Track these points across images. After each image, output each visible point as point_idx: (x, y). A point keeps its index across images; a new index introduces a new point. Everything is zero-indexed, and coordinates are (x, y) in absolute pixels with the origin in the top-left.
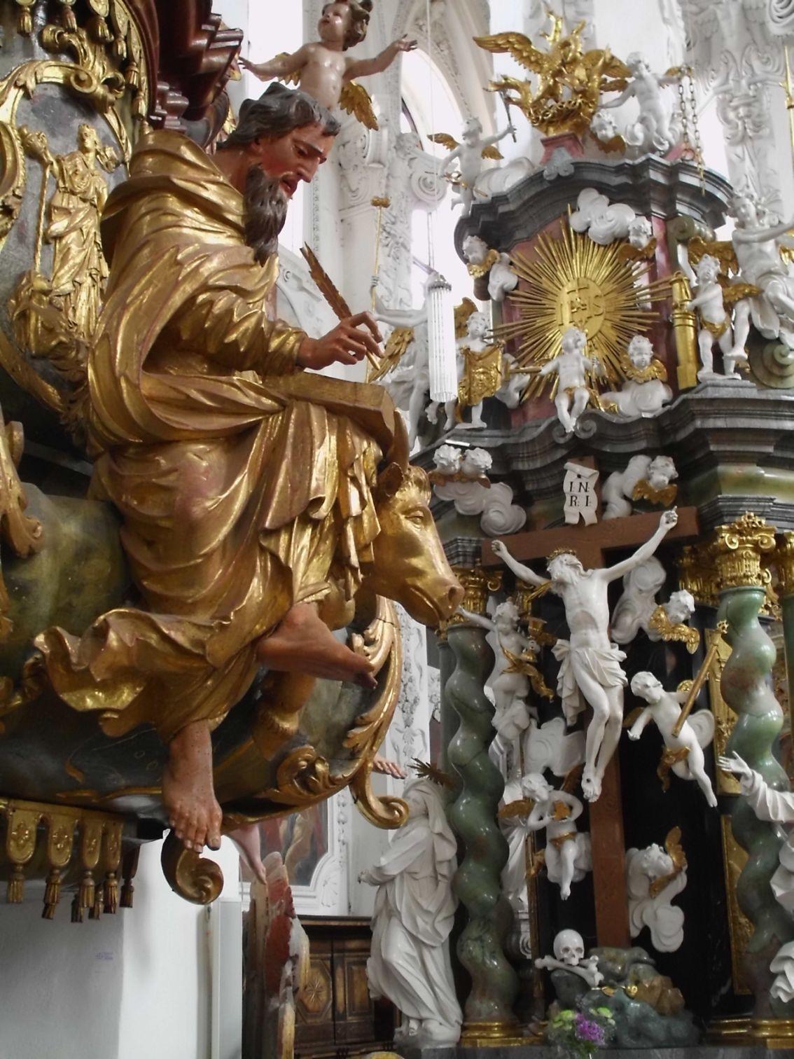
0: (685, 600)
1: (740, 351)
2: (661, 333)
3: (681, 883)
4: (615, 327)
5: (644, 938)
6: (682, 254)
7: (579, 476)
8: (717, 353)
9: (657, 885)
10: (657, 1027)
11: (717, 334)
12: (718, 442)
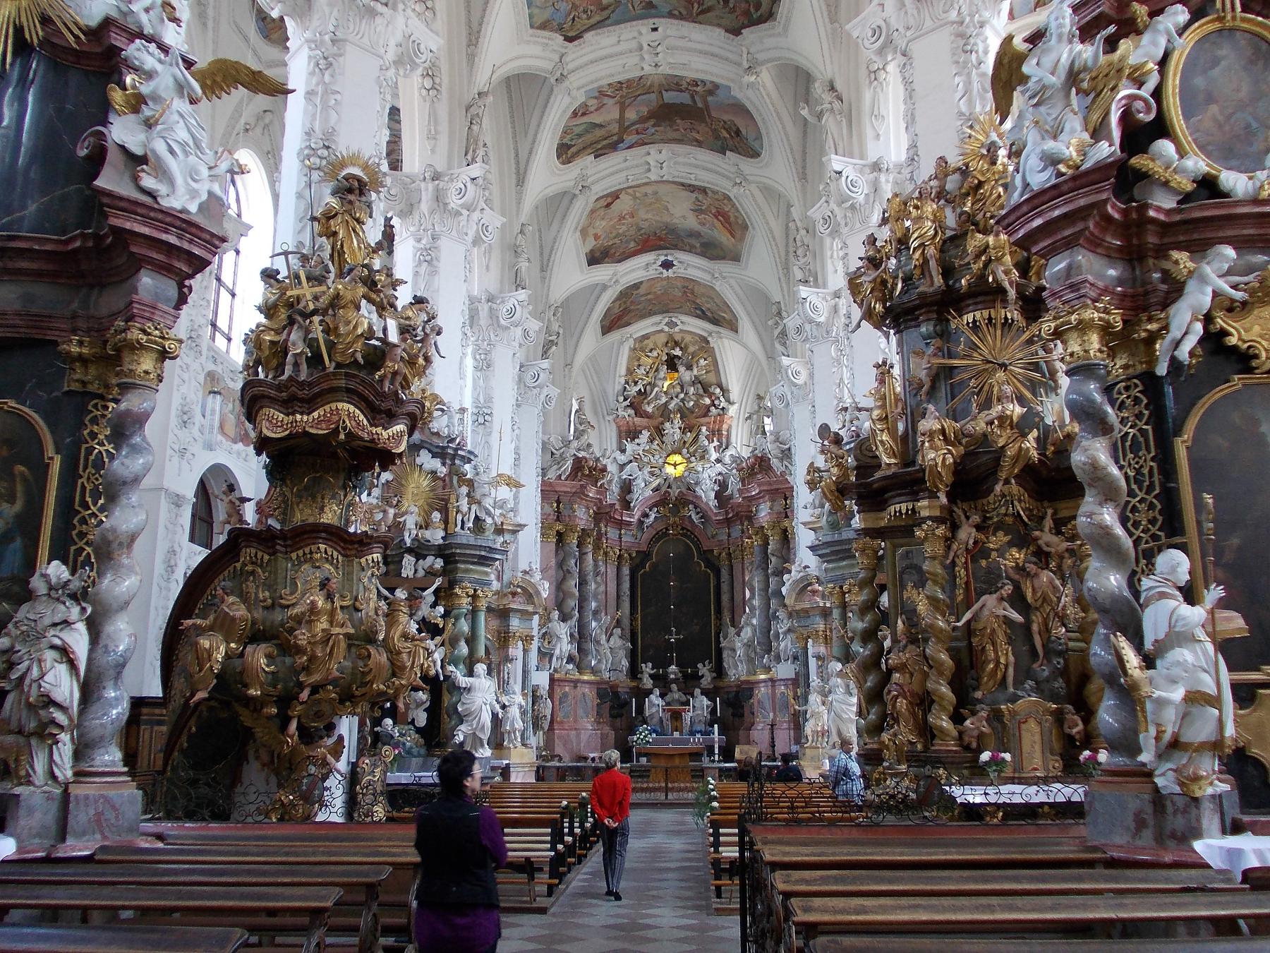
0: (441, 609)
1: (471, 525)
2: (445, 511)
3: (428, 704)
5: (413, 722)
6: (455, 479)
7: (408, 560)
9: (419, 705)
10: (415, 751)
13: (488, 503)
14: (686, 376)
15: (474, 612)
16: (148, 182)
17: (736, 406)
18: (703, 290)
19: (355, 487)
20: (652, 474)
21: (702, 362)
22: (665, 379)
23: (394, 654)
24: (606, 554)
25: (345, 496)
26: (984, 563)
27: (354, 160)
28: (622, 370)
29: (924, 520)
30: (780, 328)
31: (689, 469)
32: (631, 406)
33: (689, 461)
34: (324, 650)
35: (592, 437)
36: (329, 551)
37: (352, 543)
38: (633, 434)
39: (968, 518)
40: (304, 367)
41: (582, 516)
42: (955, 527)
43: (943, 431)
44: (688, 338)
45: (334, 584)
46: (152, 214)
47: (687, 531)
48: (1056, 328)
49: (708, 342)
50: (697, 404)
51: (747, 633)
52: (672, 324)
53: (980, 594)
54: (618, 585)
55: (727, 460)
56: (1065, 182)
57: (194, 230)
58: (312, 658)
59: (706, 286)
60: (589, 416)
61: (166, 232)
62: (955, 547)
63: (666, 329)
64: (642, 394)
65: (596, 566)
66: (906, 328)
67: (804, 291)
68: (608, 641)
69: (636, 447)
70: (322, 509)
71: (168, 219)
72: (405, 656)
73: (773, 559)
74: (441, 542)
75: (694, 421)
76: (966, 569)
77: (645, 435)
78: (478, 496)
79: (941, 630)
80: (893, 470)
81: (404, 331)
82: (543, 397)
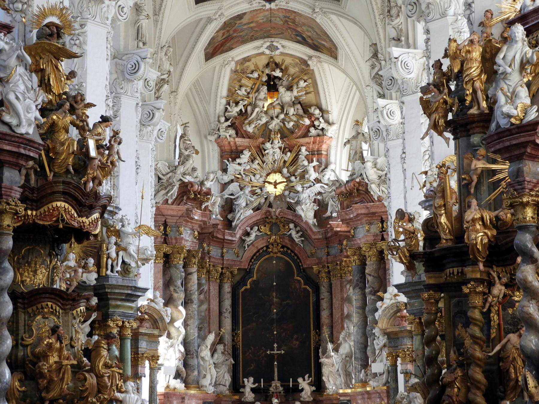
1: (119, 268)
4: (83, 252)
8: (112, 266)
11: (113, 261)
12: (111, 295)
13: (132, 249)
14: (287, 96)
15: (122, 338)
16: (7, 118)
17: (334, 128)
18: (303, 20)
19: (57, 255)
20: (253, 193)
21: (302, 84)
22: (265, 99)
23: (100, 377)
24: (209, 272)
25: (51, 262)
26: (510, 311)
27: (52, 11)
28: (224, 92)
29: (469, 281)
30: (376, 69)
31: (290, 188)
32: (232, 126)
33: (288, 180)
34: (58, 376)
35: (195, 161)
36: (54, 306)
37: (68, 300)
38: (234, 154)
39: (500, 278)
40: (33, 177)
41: (188, 238)
42: (491, 284)
43: (482, 219)
44: (288, 61)
45: (61, 330)
46: (13, 139)
47: (289, 249)
48: (511, 203)
49: (308, 65)
50: (297, 125)
51: (345, 349)
52: (272, 48)
53: (507, 332)
54: (220, 302)
55: (325, 180)
56: (514, 129)
57: (31, 144)
58: (51, 381)
59: (306, 18)
60: (194, 140)
61: (19, 147)
62: (490, 299)
63: (267, 52)
64: (243, 114)
65: (200, 285)
66: (461, 137)
67: (396, 51)
68: (212, 356)
69: (238, 167)
70: (35, 272)
71: (21, 140)
72: (106, 379)
73: (369, 278)
74: (95, 282)
75: (294, 141)
76: (498, 315)
77: (246, 156)
78: (123, 245)
79: (479, 359)
80: (450, 244)
81: (99, 147)
82: (155, 132)
